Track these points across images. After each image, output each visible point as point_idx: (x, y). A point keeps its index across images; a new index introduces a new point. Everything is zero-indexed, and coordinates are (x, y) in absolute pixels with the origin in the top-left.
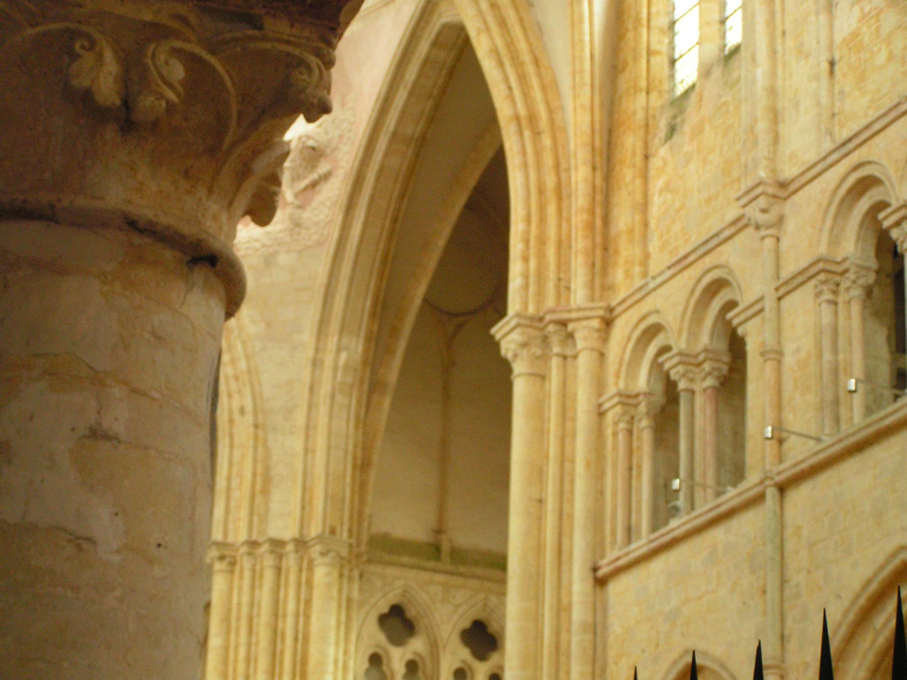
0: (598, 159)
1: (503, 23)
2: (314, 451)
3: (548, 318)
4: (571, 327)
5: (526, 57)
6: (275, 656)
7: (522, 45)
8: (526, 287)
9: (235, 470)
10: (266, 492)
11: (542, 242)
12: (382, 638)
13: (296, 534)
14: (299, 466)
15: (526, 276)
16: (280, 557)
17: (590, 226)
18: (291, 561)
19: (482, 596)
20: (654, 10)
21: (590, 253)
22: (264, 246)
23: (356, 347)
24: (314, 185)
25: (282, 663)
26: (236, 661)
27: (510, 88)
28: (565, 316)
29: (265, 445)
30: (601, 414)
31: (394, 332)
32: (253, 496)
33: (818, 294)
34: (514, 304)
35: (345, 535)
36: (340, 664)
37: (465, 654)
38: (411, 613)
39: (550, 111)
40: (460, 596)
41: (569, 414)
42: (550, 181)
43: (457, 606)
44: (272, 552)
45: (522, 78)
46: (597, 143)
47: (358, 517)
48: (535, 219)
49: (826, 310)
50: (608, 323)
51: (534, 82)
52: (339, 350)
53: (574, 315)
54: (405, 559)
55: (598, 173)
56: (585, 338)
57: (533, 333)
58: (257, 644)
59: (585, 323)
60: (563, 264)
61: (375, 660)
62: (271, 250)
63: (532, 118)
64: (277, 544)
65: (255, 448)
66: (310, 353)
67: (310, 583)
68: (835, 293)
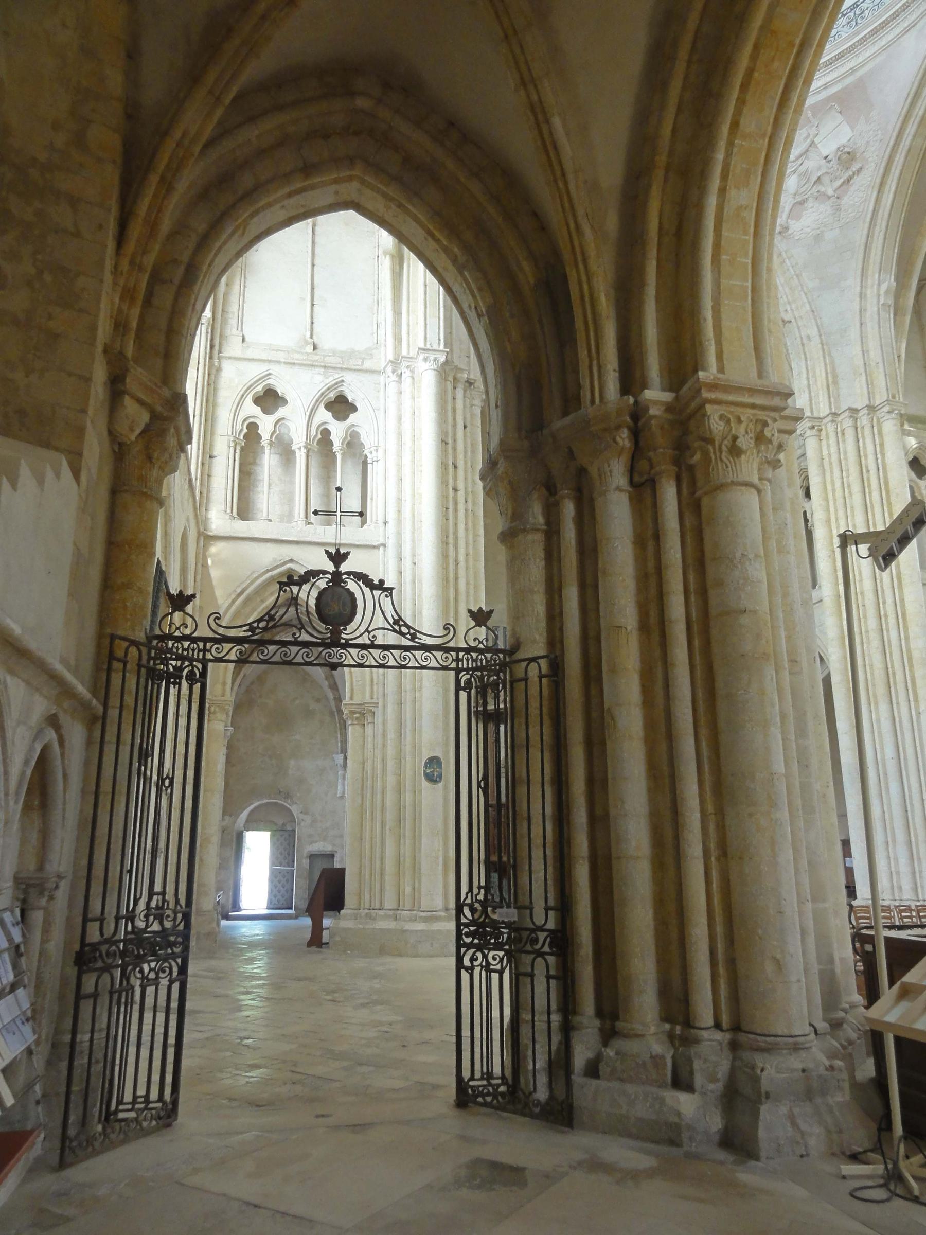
9: (811, 374)
10: (835, 382)
13: (867, 403)
16: (856, 420)
18: (864, 420)
22: (813, 230)
23: (889, 282)
24: (849, 180)
25: (869, 486)
26: (834, 491)
29: (830, 354)
44: (851, 417)
58: (848, 477)
64: (854, 411)
65: (824, 357)
66: (858, 289)
67: (880, 433)
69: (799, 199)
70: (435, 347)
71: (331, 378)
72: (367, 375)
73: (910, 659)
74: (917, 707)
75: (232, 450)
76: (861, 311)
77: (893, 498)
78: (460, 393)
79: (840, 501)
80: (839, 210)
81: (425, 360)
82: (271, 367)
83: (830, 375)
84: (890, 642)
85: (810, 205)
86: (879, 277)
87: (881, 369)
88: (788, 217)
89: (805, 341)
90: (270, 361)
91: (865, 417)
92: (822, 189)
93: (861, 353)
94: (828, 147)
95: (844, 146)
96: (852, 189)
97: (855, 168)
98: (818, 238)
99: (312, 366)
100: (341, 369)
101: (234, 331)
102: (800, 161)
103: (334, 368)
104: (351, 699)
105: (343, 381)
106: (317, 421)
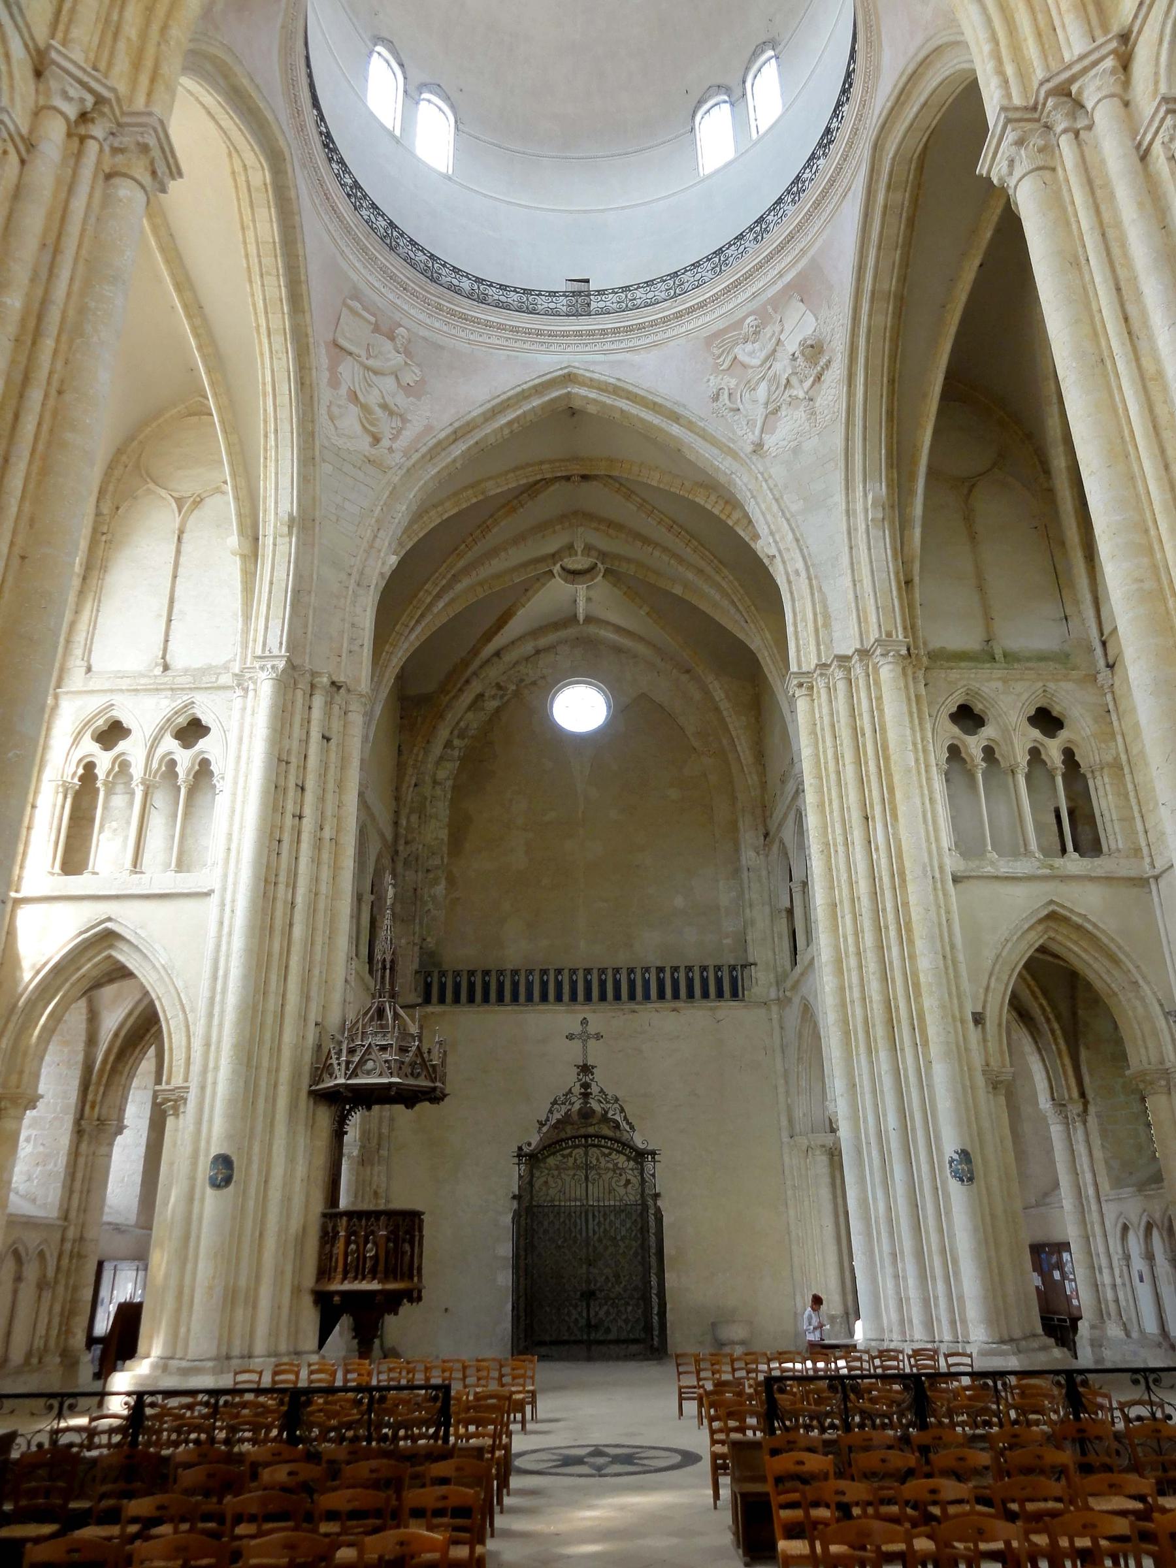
2: (861, 581)
4: (1074, 89)
6: (857, 748)
9: (799, 618)
10: (827, 625)
12: (956, 730)
14: (851, 596)
16: (849, 670)
18: (858, 670)
19: (1041, 684)
24: (818, 378)
26: (826, 763)
28: (1066, 75)
30: (1144, 156)
31: (912, 477)
32: (817, 630)
35: (901, 637)
36: (920, 746)
37: (1036, 733)
38: (978, 707)
40: (1019, 687)
41: (1098, 182)
43: (1019, 695)
44: (840, 667)
47: (911, 628)
50: (1125, 64)
52: (865, 495)
53: (1077, 68)
54: (963, 664)
57: (1028, 126)
58: (841, 745)
61: (954, 752)
62: (796, 443)
64: (843, 659)
65: (812, 594)
67: (877, 683)
69: (771, 407)
70: (276, 652)
71: (179, 701)
72: (219, 692)
73: (917, 985)
74: (926, 1053)
75: (61, 796)
76: (849, 533)
77: (893, 768)
78: (318, 701)
79: (833, 777)
80: (813, 413)
81: (262, 668)
82: (113, 697)
83: (819, 616)
84: (891, 963)
85: (784, 413)
86: (864, 487)
87: (872, 601)
88: (762, 432)
89: (792, 578)
90: (111, 691)
91: (858, 665)
92: (795, 393)
93: (850, 584)
94: (792, 345)
95: (805, 340)
96: (825, 386)
98: (796, 451)
99: (157, 690)
100: (190, 689)
101: (79, 662)
102: (768, 365)
103: (183, 689)
104: (168, 1083)
105: (193, 703)
106: (160, 751)
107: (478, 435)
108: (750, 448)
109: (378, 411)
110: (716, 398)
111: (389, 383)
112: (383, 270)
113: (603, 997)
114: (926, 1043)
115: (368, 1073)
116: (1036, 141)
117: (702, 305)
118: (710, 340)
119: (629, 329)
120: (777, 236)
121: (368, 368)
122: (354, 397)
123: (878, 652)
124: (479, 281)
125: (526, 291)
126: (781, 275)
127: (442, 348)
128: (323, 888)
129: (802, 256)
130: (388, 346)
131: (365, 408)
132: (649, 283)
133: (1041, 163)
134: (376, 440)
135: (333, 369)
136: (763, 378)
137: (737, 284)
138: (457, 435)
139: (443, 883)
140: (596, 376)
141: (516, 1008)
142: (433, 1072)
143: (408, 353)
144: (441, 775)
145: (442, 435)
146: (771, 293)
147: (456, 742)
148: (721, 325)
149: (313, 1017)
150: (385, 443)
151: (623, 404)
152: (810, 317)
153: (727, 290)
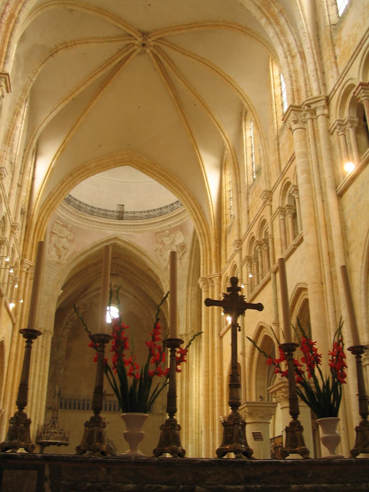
0: (217, 240)
1: (196, 213)
3: (208, 277)
4: (213, 279)
5: (201, 219)
7: (200, 217)
8: (203, 271)
11: (207, 261)
15: (203, 269)
17: (216, 256)
20: (227, 205)
21: (216, 262)
24: (183, 254)
27: (198, 227)
33: (247, 264)
34: (201, 276)
39: (207, 231)
42: (208, 246)
45: (201, 224)
46: (217, 236)
48: (205, 256)
49: (249, 268)
51: (203, 224)
52: (192, 291)
55: (217, 244)
56: (216, 282)
57: (205, 282)
59: (215, 278)
60: (211, 265)
63: (203, 233)
68: (251, 264)
91: (185, 338)
97: (185, 250)
102: (171, 245)
107: (88, 253)
108: (164, 268)
109: (62, 249)
110: (156, 251)
111: (65, 240)
112: (67, 210)
113: (110, 410)
114: (188, 439)
115: (51, 439)
116: (206, 286)
117: (155, 223)
118: (157, 233)
119: (134, 225)
120: (176, 212)
121: (59, 237)
122: (55, 245)
123: (190, 336)
124: (92, 207)
125: (106, 210)
126: (176, 223)
127: (80, 229)
128: (40, 389)
129: (182, 220)
130: (65, 229)
131: (58, 249)
132: (141, 212)
133: (206, 290)
134: (60, 257)
135: (50, 240)
136: (169, 249)
137: (164, 220)
138: (82, 254)
139: (63, 369)
140: (123, 239)
141: (84, 411)
142: (67, 439)
143: (71, 231)
144: (64, 334)
145: (78, 254)
146: (173, 226)
147: (70, 323)
148: (159, 230)
149: (37, 423)
150: (62, 258)
151: (130, 248)
152: (182, 236)
153: (162, 221)
